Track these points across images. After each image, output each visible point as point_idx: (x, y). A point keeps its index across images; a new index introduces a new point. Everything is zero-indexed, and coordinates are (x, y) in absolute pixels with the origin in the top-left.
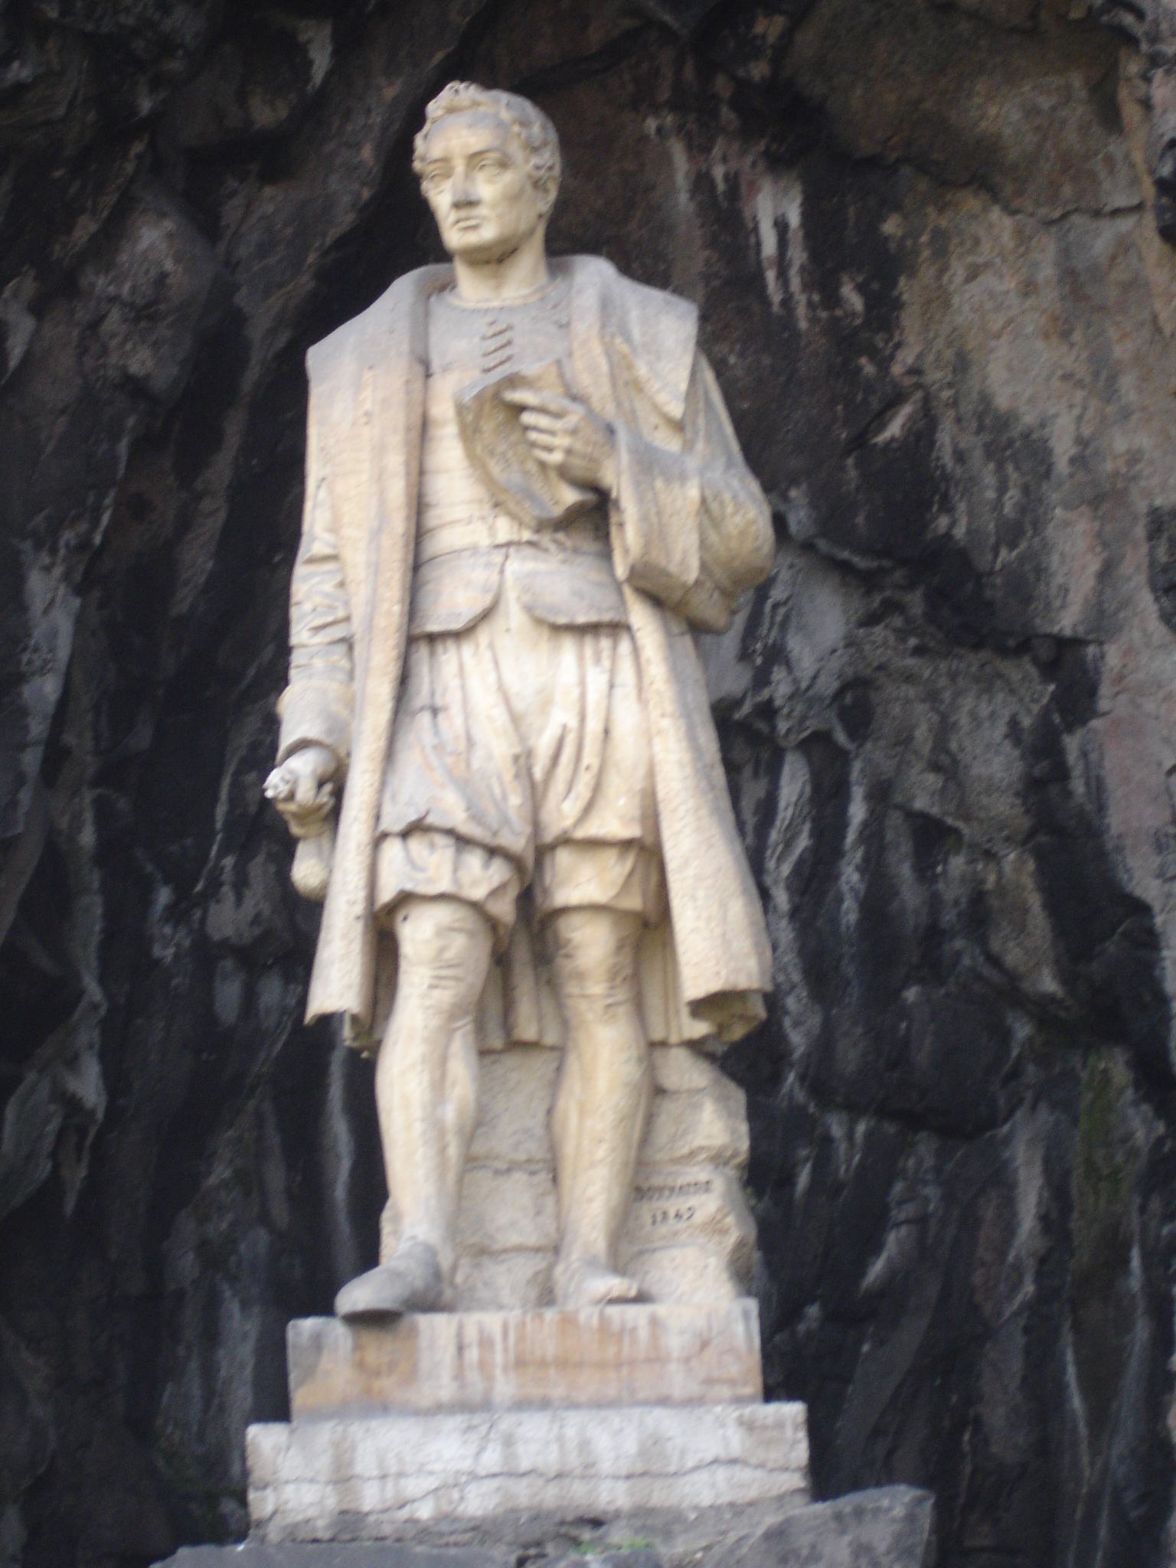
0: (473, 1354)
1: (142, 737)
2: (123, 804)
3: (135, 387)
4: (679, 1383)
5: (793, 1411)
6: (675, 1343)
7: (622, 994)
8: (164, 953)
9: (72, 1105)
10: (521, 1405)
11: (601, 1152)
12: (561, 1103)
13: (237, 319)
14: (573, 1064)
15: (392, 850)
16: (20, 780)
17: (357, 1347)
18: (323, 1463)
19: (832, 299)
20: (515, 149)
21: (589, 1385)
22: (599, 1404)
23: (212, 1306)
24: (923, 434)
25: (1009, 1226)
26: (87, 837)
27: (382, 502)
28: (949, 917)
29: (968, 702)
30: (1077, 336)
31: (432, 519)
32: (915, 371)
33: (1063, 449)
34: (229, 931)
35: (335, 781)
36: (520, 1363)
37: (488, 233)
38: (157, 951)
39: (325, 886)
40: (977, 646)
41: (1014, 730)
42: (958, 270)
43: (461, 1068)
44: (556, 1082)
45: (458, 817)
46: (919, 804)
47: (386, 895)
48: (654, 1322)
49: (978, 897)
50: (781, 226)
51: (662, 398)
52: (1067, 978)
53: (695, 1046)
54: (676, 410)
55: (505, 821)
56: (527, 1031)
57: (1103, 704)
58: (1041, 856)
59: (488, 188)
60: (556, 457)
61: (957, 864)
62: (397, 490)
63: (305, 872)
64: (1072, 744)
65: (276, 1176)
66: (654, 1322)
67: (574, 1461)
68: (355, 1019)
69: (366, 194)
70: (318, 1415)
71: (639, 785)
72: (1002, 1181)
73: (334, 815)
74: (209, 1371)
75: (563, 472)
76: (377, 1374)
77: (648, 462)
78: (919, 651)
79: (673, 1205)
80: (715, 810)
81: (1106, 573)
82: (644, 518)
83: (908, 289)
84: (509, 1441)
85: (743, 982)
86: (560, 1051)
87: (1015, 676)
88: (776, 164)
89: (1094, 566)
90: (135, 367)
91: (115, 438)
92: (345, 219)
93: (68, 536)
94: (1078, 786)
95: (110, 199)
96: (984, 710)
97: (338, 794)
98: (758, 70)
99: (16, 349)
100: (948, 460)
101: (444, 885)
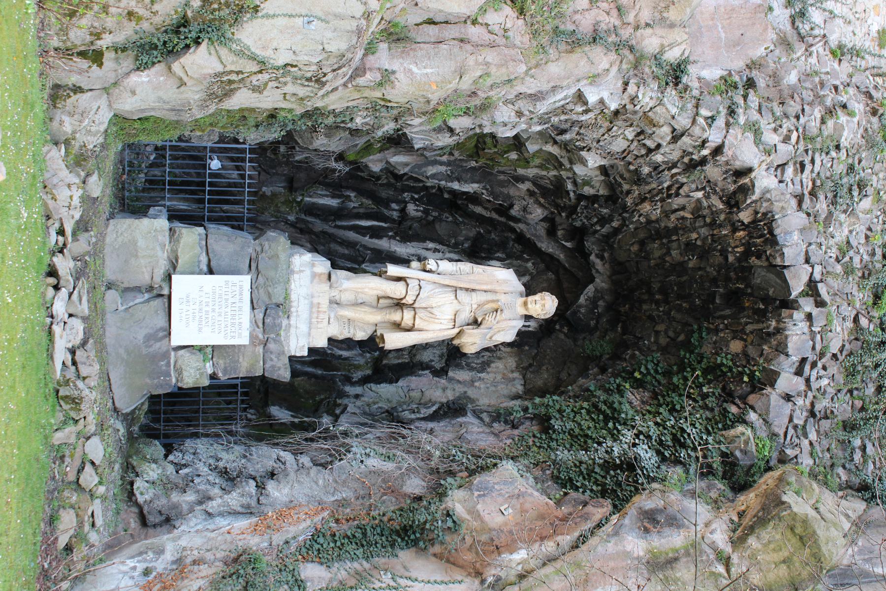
1: (446, 196)
2: (434, 191)
3: (511, 206)
5: (306, 354)
12: (367, 309)
23: (339, 197)
33: (482, 375)
37: (529, 306)
41: (432, 361)
44: (371, 306)
47: (408, 281)
52: (385, 365)
56: (381, 301)
64: (427, 372)
65: (362, 211)
68: (386, 272)
73: (425, 271)
74: (327, 196)
75: (484, 319)
81: (459, 382)
86: (377, 307)
89: (461, 379)
92: (539, 245)
93: (484, 191)
97: (428, 271)
98: (557, 327)
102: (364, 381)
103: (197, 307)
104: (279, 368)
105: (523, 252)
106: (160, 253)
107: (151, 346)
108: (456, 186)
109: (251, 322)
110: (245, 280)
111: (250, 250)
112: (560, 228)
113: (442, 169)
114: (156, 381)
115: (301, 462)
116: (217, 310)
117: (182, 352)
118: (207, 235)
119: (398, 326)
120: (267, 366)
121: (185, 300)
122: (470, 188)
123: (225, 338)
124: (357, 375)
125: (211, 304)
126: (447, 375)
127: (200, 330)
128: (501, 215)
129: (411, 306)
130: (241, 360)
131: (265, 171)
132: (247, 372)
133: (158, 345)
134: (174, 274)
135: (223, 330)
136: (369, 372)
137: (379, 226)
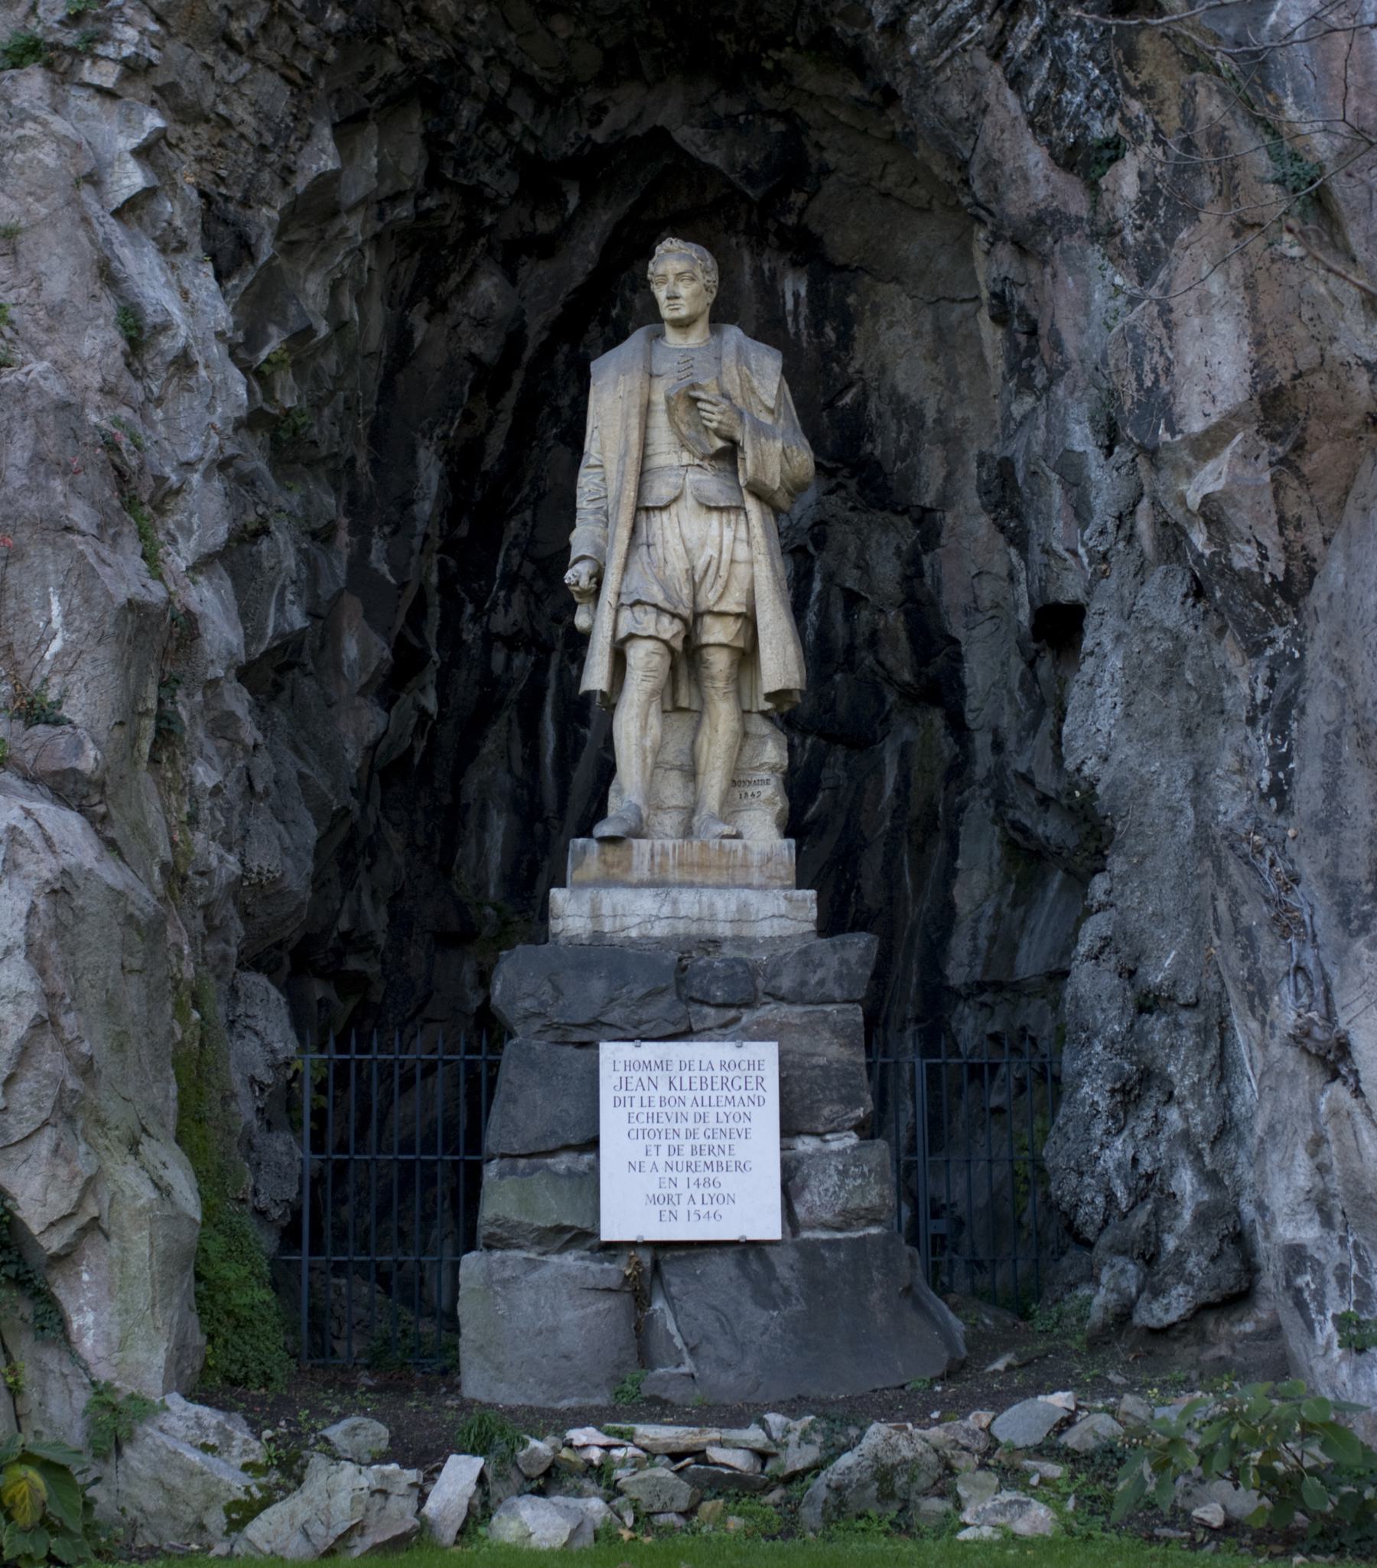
0: (657, 859)
1: (463, 530)
3: (473, 359)
4: (756, 878)
5: (811, 894)
6: (755, 859)
7: (731, 688)
8: (469, 637)
9: (423, 712)
10: (681, 885)
11: (719, 763)
12: (703, 740)
13: (523, 326)
14: (706, 719)
15: (626, 615)
16: (412, 553)
17: (602, 853)
18: (586, 909)
19: (820, 333)
20: (698, 272)
21: (713, 877)
22: (718, 886)
23: (484, 809)
24: (861, 403)
25: (880, 794)
26: (434, 579)
27: (627, 441)
28: (859, 641)
29: (876, 536)
30: (940, 360)
31: (650, 451)
32: (859, 371)
33: (930, 415)
34: (500, 629)
35: (598, 577)
36: (681, 865)
37: (683, 312)
38: (465, 636)
39: (591, 627)
40: (882, 509)
42: (883, 323)
43: (654, 721)
44: (697, 729)
45: (659, 598)
46: (847, 585)
47: (622, 634)
48: (745, 847)
49: (874, 633)
50: (796, 295)
51: (764, 397)
52: (917, 675)
53: (764, 714)
54: (771, 404)
55: (681, 601)
56: (684, 702)
57: (943, 541)
58: (907, 614)
59: (684, 290)
60: (714, 425)
61: (865, 615)
62: (635, 436)
63: (581, 620)
64: (926, 560)
65: (517, 750)
66: (745, 847)
67: (706, 913)
68: (602, 693)
69: (591, 267)
70: (583, 885)
71: (746, 586)
72: (878, 769)
73: (595, 594)
74: (480, 843)
75: (717, 433)
76: (612, 866)
77: (759, 429)
78: (853, 509)
79: (755, 790)
80: (782, 602)
82: (756, 457)
83: (857, 331)
84: (675, 902)
85: (792, 686)
86: (700, 713)
87: (901, 525)
88: (795, 264)
89: (943, 473)
90: (475, 350)
91: (462, 384)
92: (579, 279)
93: (438, 432)
94: (928, 581)
95: (467, 266)
96: (884, 540)
99: (418, 337)
100: (873, 416)
101: (651, 632)
102: (958, 727)
103: (682, 1177)
104: (844, 962)
105: (605, 320)
106: (546, 1272)
107: (786, 1291)
108: (425, 508)
109: (723, 1038)
110: (613, 1056)
111: (539, 1045)
112: (528, 228)
113: (377, 546)
114: (877, 1276)
115: (1103, 898)
116: (691, 1125)
117: (800, 1210)
118: (503, 1156)
119: (747, 656)
120: (837, 993)
121: (666, 1207)
122: (430, 470)
123: (760, 1102)
124: (948, 747)
125: (675, 1142)
126: (932, 510)
127: (741, 1167)
128: (508, 385)
129: (692, 624)
130: (822, 1061)
131: (420, 1009)
132: (852, 1044)
133: (783, 1271)
134: (598, 1235)
135: (741, 1109)
136: (937, 718)
137: (555, 708)
